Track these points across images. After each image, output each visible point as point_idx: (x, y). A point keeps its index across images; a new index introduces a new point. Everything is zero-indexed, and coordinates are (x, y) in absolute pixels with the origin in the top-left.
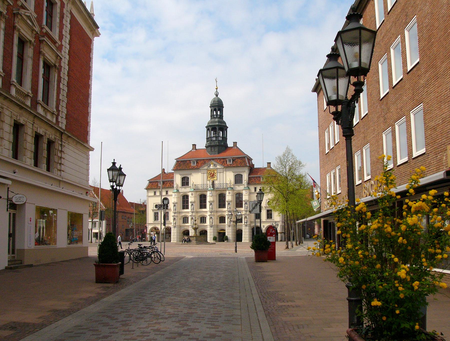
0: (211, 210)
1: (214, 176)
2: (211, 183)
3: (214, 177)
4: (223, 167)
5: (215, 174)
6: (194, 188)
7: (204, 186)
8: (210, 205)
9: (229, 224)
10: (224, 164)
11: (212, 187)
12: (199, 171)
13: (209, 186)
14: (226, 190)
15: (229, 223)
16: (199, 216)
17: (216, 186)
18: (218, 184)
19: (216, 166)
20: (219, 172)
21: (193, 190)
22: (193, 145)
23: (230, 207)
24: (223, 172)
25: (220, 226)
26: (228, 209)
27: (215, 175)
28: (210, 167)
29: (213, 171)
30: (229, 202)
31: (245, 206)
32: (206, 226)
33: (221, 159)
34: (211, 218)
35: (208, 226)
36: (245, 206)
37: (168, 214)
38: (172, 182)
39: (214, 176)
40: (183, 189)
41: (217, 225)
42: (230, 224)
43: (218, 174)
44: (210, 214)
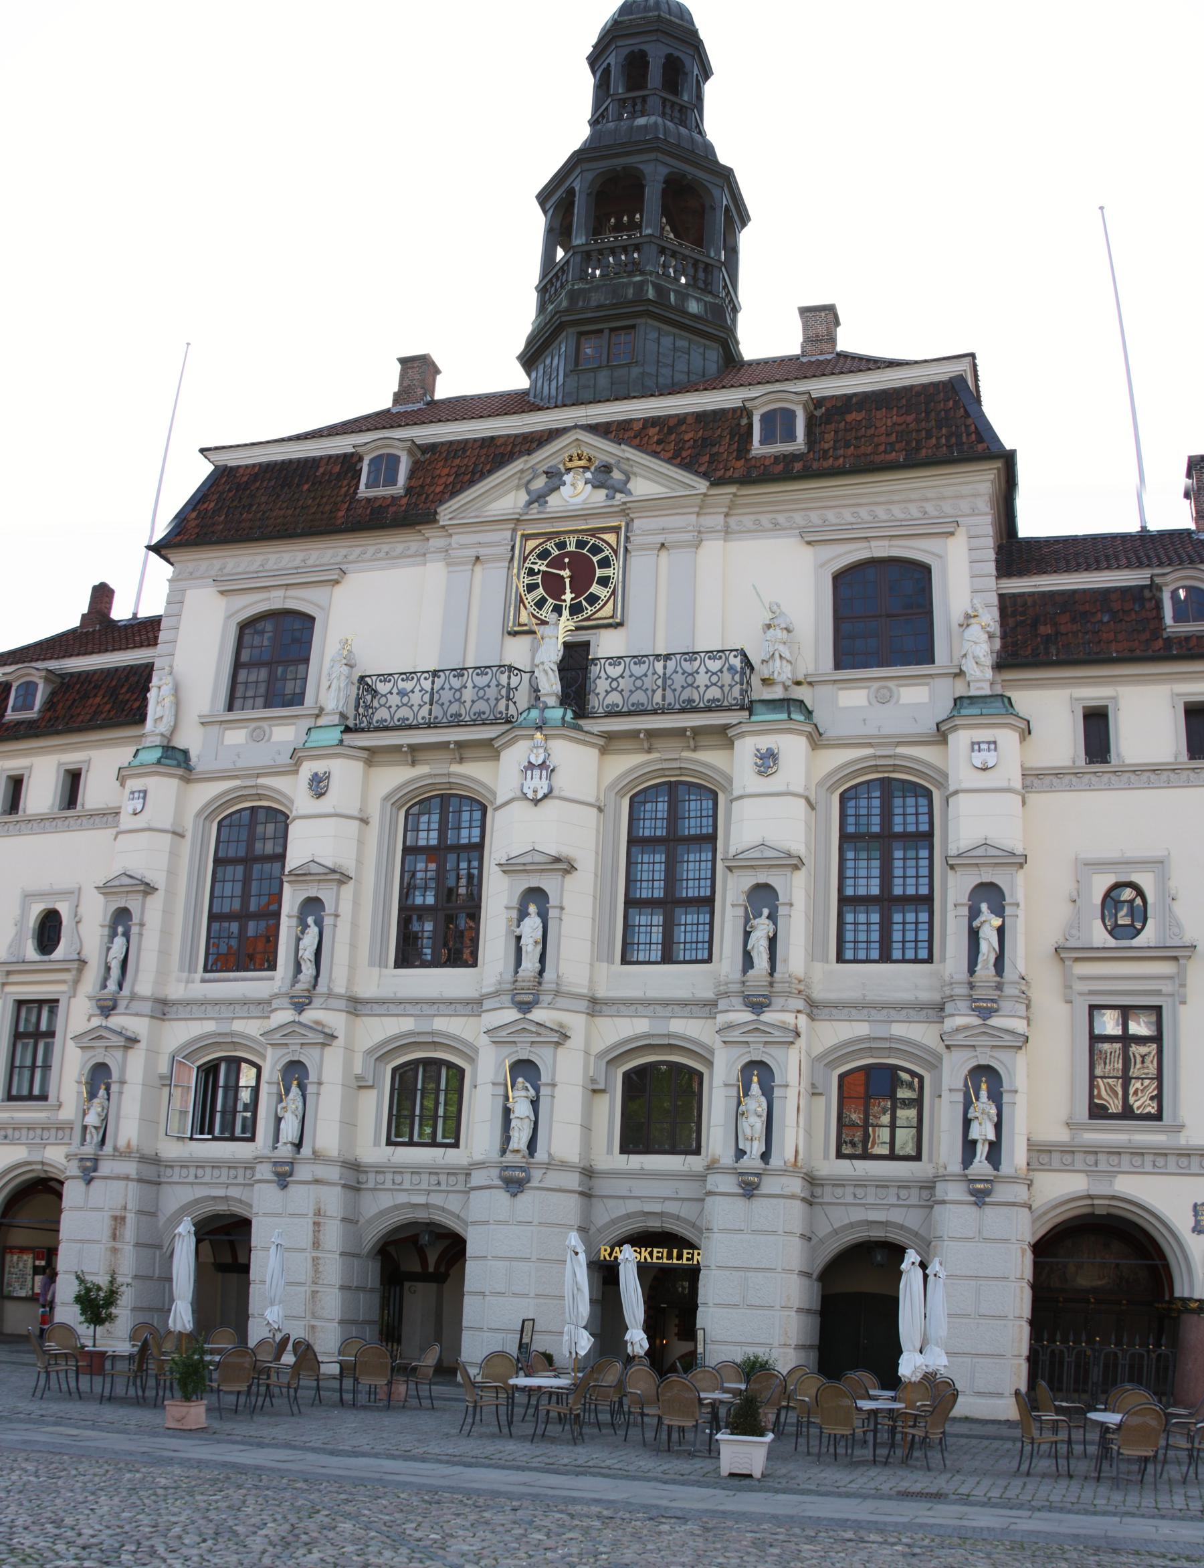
0: (530, 964)
1: (595, 589)
2: (551, 652)
3: (593, 599)
4: (702, 485)
5: (605, 563)
6: (351, 723)
7: (468, 694)
8: (523, 914)
9: (752, 1161)
10: (714, 459)
11: (564, 701)
12: (436, 541)
13: (522, 698)
14: (724, 736)
15: (758, 1148)
16: (381, 1054)
17: (603, 692)
18: (639, 659)
19: (623, 490)
20: (646, 548)
21: (335, 735)
22: (404, 361)
23: (773, 941)
24: (697, 544)
25: (620, 1187)
26: (748, 961)
27: (604, 582)
28: (553, 500)
29: (581, 544)
30: (762, 878)
31: (974, 936)
32: (452, 1172)
33: (681, 419)
34: (525, 1069)
35: (478, 1178)
36: (974, 936)
37: (53, 1012)
38: (141, 677)
39: (595, 589)
40: (236, 737)
41: (588, 1173)
42: (765, 1156)
43: (640, 563)
44: (512, 1015)
